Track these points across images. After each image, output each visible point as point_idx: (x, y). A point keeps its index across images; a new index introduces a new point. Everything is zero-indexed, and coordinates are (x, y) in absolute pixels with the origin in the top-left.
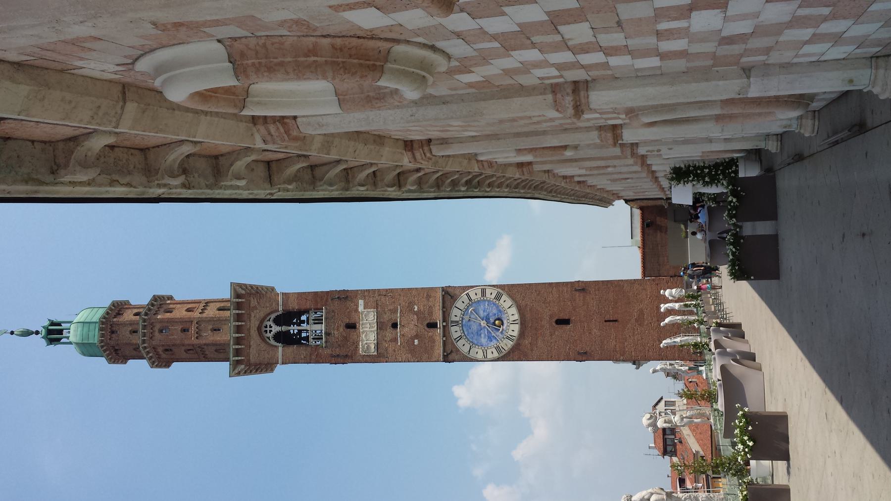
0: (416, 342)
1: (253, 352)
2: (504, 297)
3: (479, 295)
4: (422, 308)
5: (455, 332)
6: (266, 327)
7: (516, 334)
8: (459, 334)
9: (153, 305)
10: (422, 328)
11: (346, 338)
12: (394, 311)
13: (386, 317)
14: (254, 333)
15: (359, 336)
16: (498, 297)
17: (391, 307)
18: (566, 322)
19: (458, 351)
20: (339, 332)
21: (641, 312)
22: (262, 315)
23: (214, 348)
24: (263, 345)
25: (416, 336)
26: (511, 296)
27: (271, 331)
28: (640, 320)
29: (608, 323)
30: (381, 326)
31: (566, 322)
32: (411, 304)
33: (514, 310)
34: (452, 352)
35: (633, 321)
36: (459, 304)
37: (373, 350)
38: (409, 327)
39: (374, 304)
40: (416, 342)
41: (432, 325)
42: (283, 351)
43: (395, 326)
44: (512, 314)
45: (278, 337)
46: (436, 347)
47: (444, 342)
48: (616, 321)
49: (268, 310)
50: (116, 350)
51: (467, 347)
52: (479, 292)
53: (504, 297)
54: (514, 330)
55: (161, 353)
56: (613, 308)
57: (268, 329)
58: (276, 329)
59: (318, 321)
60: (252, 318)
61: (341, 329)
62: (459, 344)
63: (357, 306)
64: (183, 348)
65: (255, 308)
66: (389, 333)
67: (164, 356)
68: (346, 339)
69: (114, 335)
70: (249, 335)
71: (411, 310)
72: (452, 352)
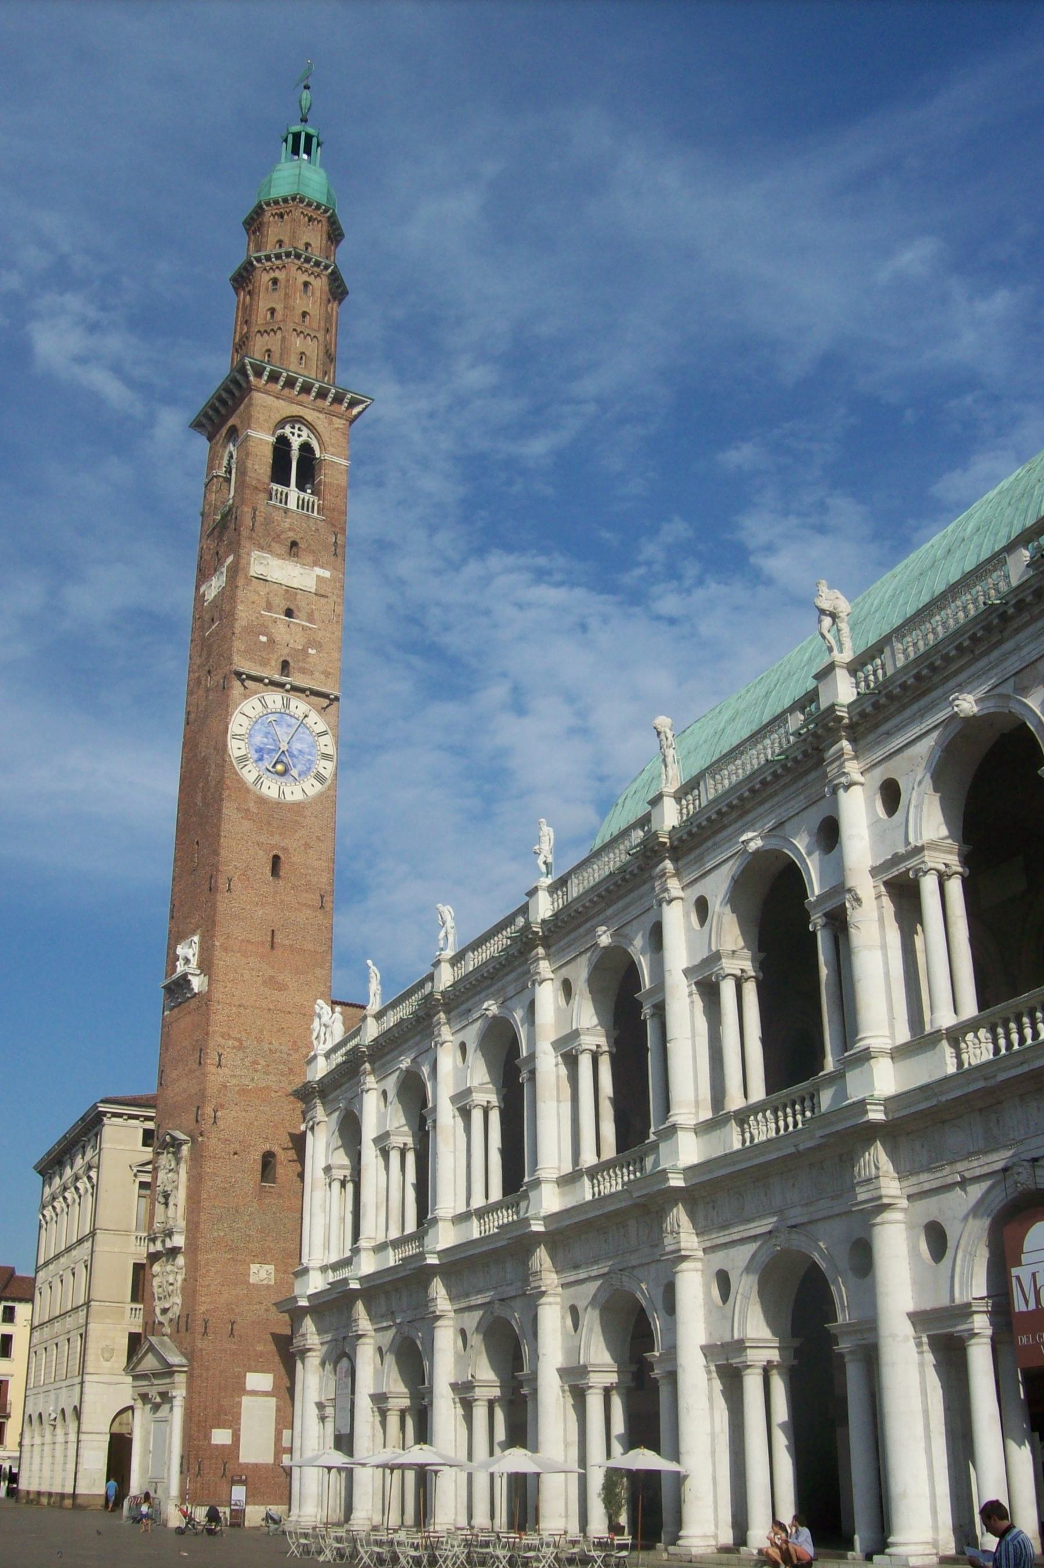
0: (263, 639)
1: (270, 400)
3: (324, 750)
4: (310, 660)
5: (275, 699)
6: (299, 429)
7: (264, 790)
8: (271, 705)
9: (339, 287)
10: (283, 653)
11: (278, 536)
12: (311, 618)
13: (302, 602)
14: (295, 410)
15: (279, 556)
16: (320, 778)
17: (316, 615)
19: (246, 697)
21: (282, 987)
22: (320, 429)
23: (276, 349)
24: (279, 418)
25: (272, 641)
26: (321, 795)
27: (293, 434)
28: (271, 982)
29: (270, 933)
30: (291, 592)
32: (319, 646)
33: (298, 796)
34: (245, 688)
36: (314, 717)
37: (256, 569)
38: (288, 635)
39: (323, 593)
40: (263, 639)
41: (285, 666)
42: (268, 443)
43: (289, 613)
45: (282, 445)
46: (252, 665)
47: (259, 680)
48: (272, 947)
49: (326, 438)
50: (281, 216)
51: (252, 713)
52: (331, 750)
53: (318, 787)
54: (271, 789)
55: (272, 275)
56: (291, 946)
57: (296, 431)
58: (296, 443)
59: (302, 504)
60: (317, 414)
61: (291, 534)
62: (254, 701)
63: (322, 567)
64: (279, 308)
65: (331, 423)
66: (280, 603)
67: (266, 278)
68: (277, 538)
69: (306, 219)
70: (292, 401)
71: (311, 643)
72: (245, 688)
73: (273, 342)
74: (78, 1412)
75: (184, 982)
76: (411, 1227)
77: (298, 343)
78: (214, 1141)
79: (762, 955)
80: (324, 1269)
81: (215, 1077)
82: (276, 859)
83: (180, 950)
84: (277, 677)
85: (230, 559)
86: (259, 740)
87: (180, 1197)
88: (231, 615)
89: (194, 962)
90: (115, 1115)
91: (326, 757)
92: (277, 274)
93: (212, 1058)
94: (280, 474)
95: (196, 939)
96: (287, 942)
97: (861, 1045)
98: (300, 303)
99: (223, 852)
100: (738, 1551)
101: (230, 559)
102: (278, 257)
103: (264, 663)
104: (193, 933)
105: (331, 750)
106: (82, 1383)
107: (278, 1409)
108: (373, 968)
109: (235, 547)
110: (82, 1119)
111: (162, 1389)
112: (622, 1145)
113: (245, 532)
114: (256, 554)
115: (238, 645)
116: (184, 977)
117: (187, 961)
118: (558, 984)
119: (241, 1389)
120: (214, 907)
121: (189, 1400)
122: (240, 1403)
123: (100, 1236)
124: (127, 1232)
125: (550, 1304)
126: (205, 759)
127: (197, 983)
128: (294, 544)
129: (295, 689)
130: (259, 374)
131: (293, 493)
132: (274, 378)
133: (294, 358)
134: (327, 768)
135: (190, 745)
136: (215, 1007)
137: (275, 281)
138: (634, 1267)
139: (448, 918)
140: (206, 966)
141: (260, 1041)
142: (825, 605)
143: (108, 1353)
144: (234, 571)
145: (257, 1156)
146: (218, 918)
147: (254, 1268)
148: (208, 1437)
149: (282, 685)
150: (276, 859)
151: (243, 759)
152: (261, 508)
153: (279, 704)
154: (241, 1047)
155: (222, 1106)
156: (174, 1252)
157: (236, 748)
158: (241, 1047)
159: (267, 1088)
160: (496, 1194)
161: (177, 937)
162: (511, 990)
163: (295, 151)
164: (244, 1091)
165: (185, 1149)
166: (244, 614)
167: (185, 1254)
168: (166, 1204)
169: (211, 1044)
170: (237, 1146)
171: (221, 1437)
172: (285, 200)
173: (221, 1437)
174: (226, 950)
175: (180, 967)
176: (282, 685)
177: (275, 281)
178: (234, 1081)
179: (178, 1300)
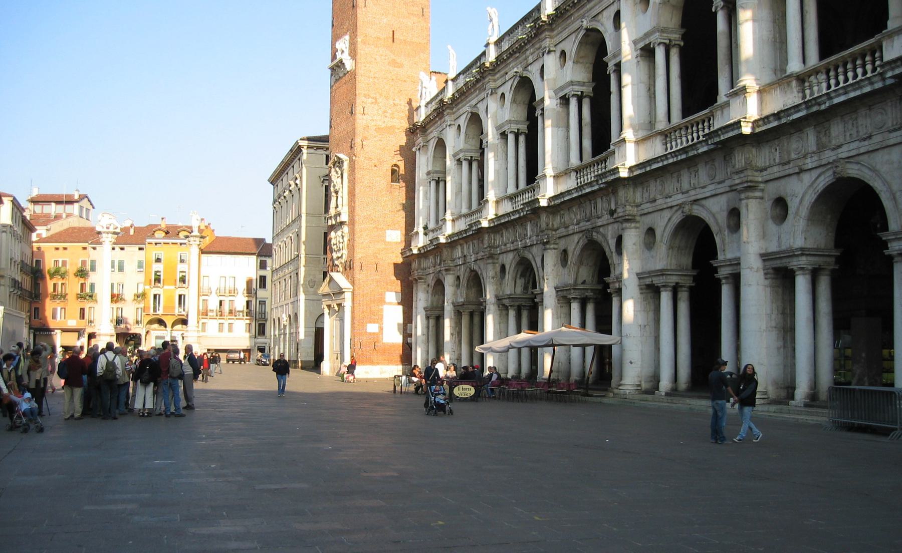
21: (401, 66)
28: (394, 63)
35: (393, 57)
76: (475, 206)
78: (362, 159)
79: (683, 31)
81: (361, 120)
83: (340, 45)
89: (347, 52)
93: (358, 110)
95: (347, 37)
96: (402, 38)
97: (741, 84)
100: (654, 393)
107: (404, 313)
108: (452, 52)
110: (291, 150)
111: (338, 302)
112: (595, 153)
116: (341, 61)
118: (558, 54)
119: (382, 301)
121: (353, 307)
122: (382, 310)
125: (550, 249)
127: (349, 64)
136: (359, 78)
138: (600, 226)
139: (493, 16)
140: (353, 54)
141: (387, 98)
145: (388, 168)
146: (358, 24)
147: (388, 232)
148: (364, 328)
154: (376, 102)
155: (366, 138)
156: (342, 223)
159: (393, 127)
160: (522, 184)
161: (335, 38)
162: (530, 60)
164: (378, 129)
165: (346, 166)
167: (348, 225)
169: (358, 101)
170: (375, 162)
171: (372, 328)
173: (372, 328)
174: (365, 43)
175: (339, 56)
178: (373, 123)
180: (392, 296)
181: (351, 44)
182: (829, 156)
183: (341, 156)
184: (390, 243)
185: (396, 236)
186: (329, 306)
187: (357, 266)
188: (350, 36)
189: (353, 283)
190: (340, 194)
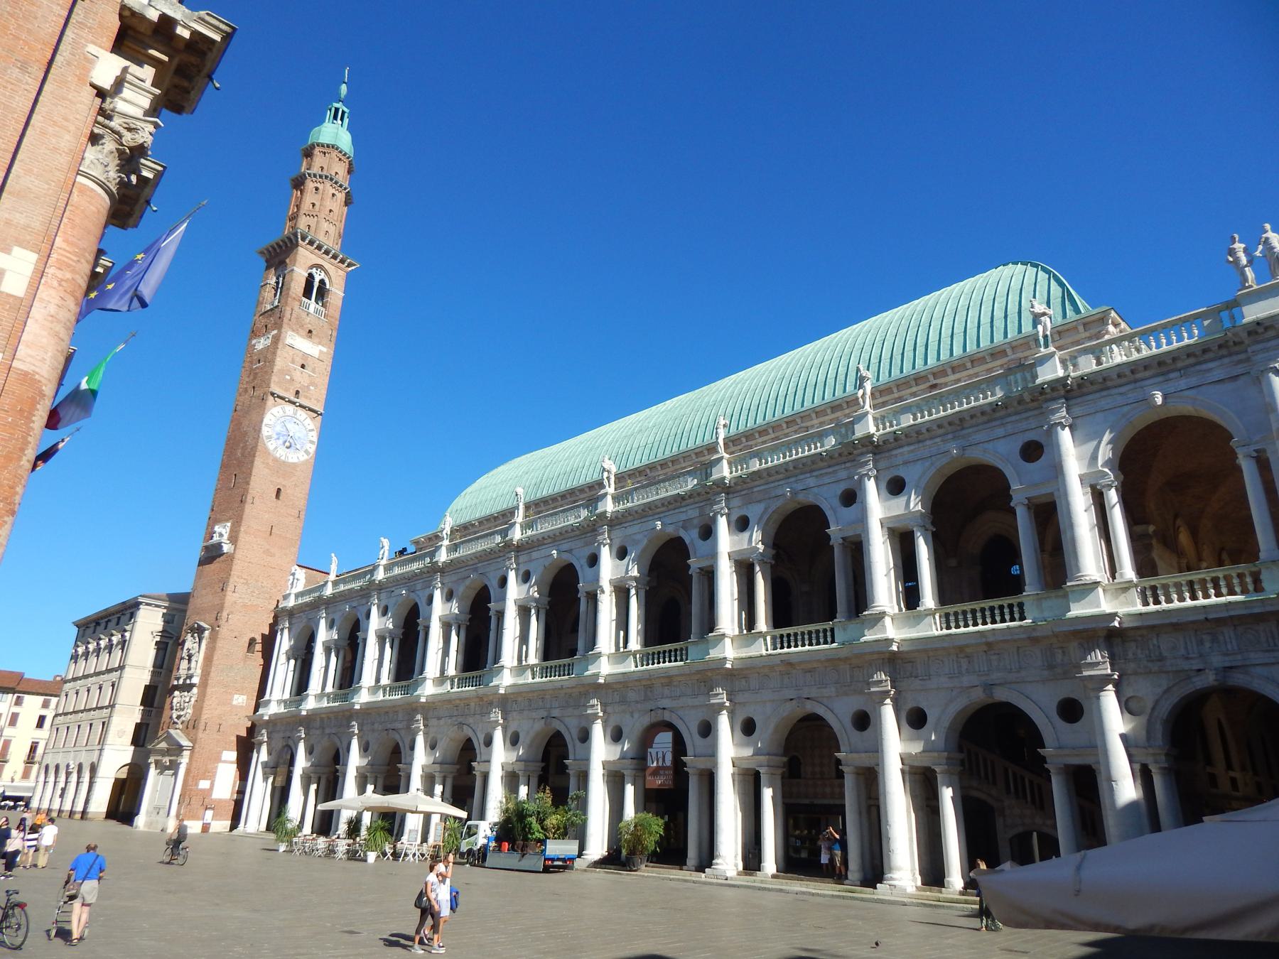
2: (306, 457)
5: (290, 409)
10: (297, 387)
13: (309, 364)
14: (320, 262)
16: (307, 452)
18: (278, 496)
20: (309, 322)
28: (267, 552)
31: (278, 496)
32: (316, 386)
33: (295, 460)
36: (309, 421)
37: (289, 341)
38: (301, 378)
41: (297, 392)
43: (303, 366)
44: (293, 457)
45: (311, 275)
54: (282, 453)
58: (317, 279)
59: (316, 311)
64: (317, 204)
73: (312, 222)
74: (93, 769)
75: (219, 546)
77: (325, 226)
80: (279, 702)
81: (230, 597)
82: (279, 490)
83: (217, 528)
84: (292, 398)
85: (275, 332)
86: (279, 428)
87: (199, 658)
88: (272, 362)
89: (226, 536)
90: (147, 604)
91: (312, 442)
92: (320, 186)
93: (230, 588)
94: (307, 293)
98: (329, 204)
99: (252, 483)
101: (275, 332)
102: (321, 177)
103: (287, 390)
104: (227, 521)
105: (315, 439)
106: (101, 750)
108: (334, 559)
109: (278, 326)
113: (285, 320)
114: (290, 333)
115: (274, 378)
117: (221, 535)
119: (218, 759)
120: (243, 510)
123: (127, 669)
124: (144, 668)
126: (246, 433)
127: (226, 548)
128: (310, 332)
129: (301, 406)
130: (303, 239)
131: (312, 305)
132: (311, 243)
133: (322, 233)
134: (312, 448)
135: (236, 424)
136: (235, 561)
137: (317, 189)
140: (234, 539)
142: (606, 466)
143: (121, 734)
144: (276, 340)
147: (236, 696)
148: (197, 784)
149: (294, 403)
150: (279, 490)
151: (269, 437)
152: (296, 308)
153: (291, 413)
156: (192, 686)
157: (265, 431)
158: (247, 584)
161: (213, 521)
162: (419, 587)
163: (335, 118)
164: (245, 606)
165: (207, 633)
166: (279, 363)
168: (189, 661)
169: (231, 580)
171: (204, 784)
172: (328, 146)
173: (204, 784)
175: (216, 538)
176: (294, 403)
177: (317, 189)
179: (190, 711)
180: (232, 755)
181: (231, 530)
182: (650, 705)
183: (202, 624)
184: (236, 706)
185: (243, 701)
186: (157, 762)
187: (202, 726)
188: (233, 525)
189: (194, 741)
190: (194, 659)
